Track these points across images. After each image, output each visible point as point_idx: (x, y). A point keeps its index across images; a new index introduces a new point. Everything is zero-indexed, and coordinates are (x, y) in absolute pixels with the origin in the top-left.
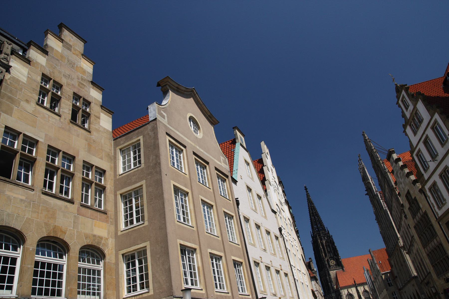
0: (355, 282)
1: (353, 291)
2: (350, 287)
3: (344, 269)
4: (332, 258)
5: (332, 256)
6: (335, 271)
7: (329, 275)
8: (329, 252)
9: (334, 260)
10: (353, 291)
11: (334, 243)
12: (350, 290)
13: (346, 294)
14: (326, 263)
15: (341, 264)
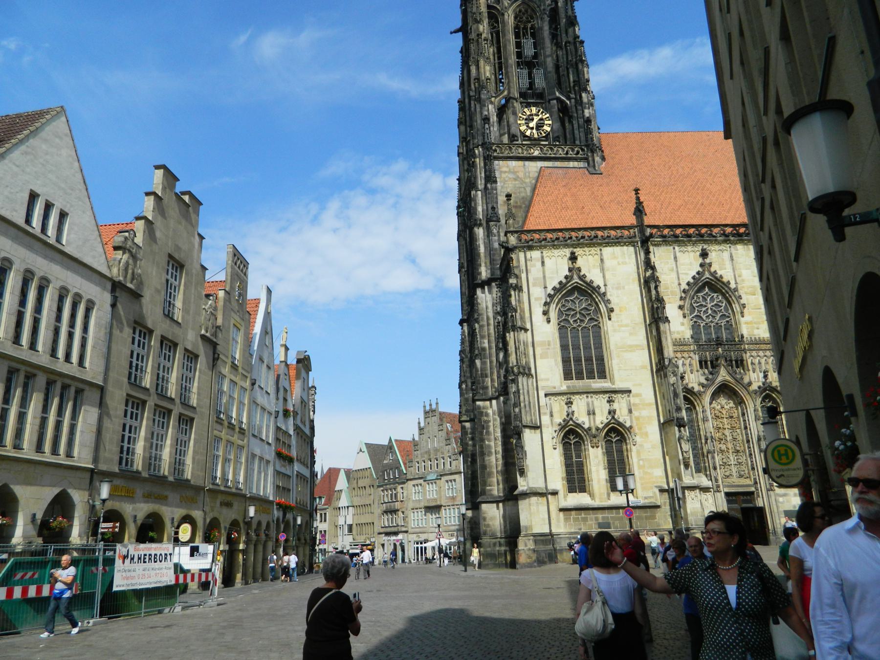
0: (639, 211)
1: (615, 270)
2: (599, 237)
3: (602, 166)
4: (532, 96)
5: (540, 82)
6: (534, 167)
7: (490, 178)
8: (529, 64)
9: (546, 110)
10: (615, 270)
11: (572, 22)
12: (590, 264)
13: (553, 283)
14: (491, 110)
15: (588, 132)
